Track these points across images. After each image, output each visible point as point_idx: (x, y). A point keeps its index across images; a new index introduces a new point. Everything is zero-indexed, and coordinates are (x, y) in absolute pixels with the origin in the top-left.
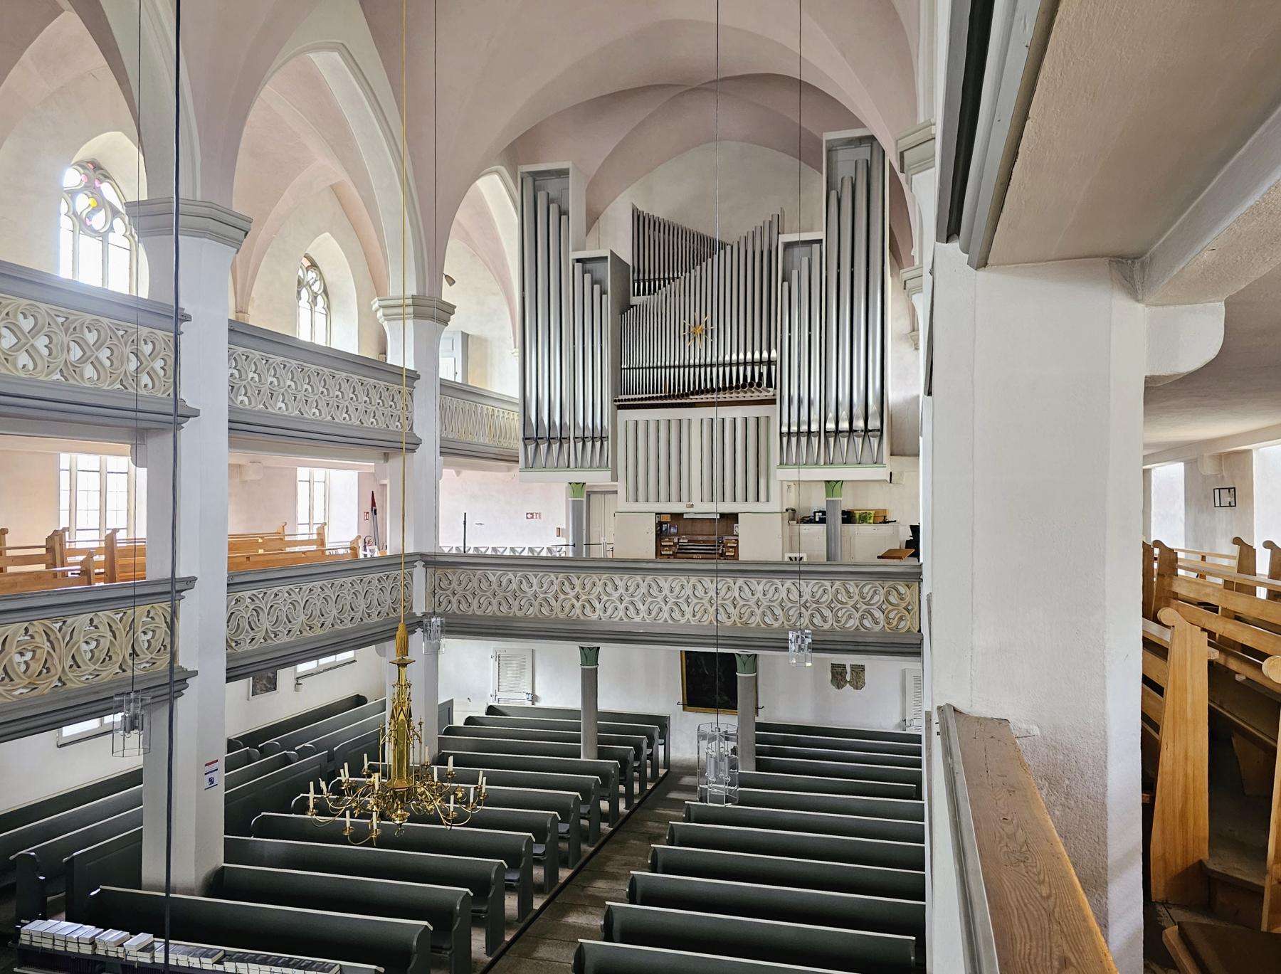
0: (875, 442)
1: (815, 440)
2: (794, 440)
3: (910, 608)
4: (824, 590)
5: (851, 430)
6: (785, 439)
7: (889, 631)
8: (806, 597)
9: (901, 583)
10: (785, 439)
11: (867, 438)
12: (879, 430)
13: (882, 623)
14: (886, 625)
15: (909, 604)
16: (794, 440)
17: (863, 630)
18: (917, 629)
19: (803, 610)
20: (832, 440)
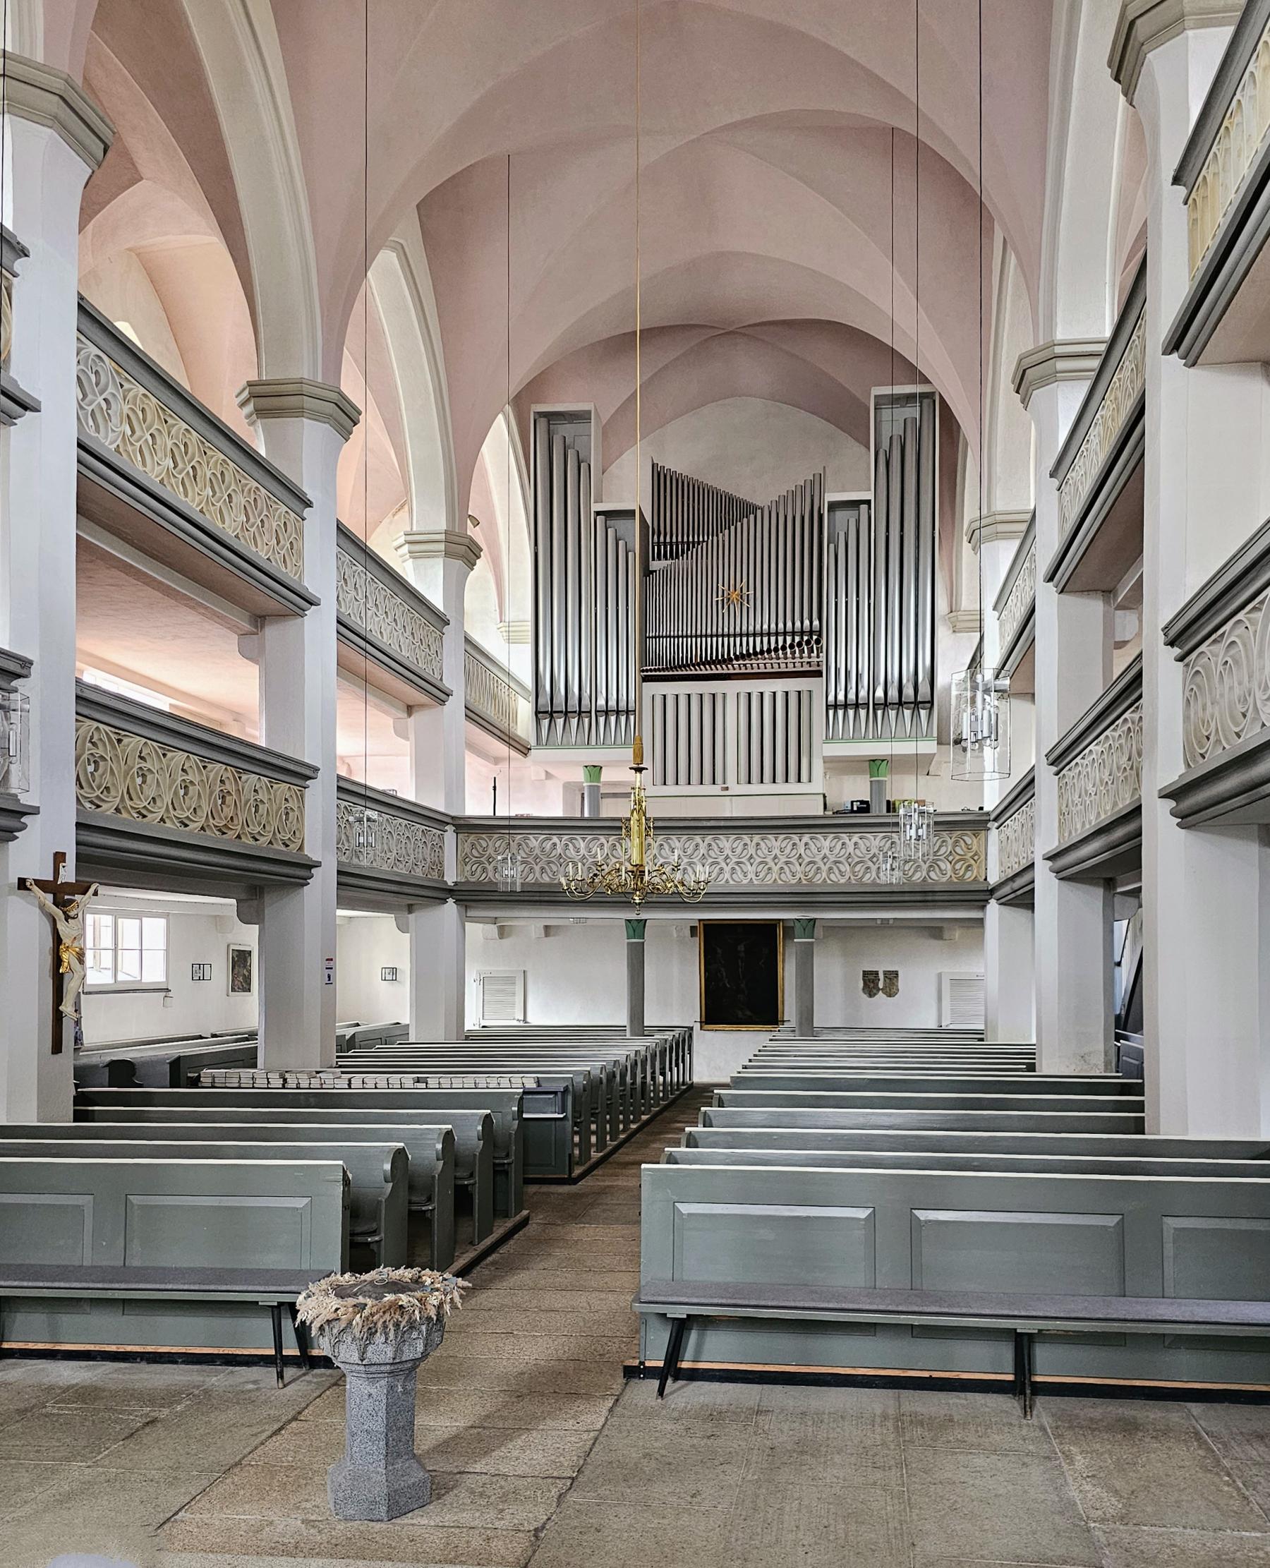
0: (923, 713)
1: (863, 712)
2: (840, 713)
3: (976, 858)
4: (892, 843)
5: (901, 703)
6: (831, 712)
7: (956, 880)
8: (874, 850)
9: (968, 832)
10: (831, 712)
11: (916, 712)
12: (928, 702)
13: (949, 873)
14: (953, 875)
15: (975, 855)
16: (840, 713)
17: (930, 881)
18: (984, 878)
19: (870, 864)
20: (879, 713)
